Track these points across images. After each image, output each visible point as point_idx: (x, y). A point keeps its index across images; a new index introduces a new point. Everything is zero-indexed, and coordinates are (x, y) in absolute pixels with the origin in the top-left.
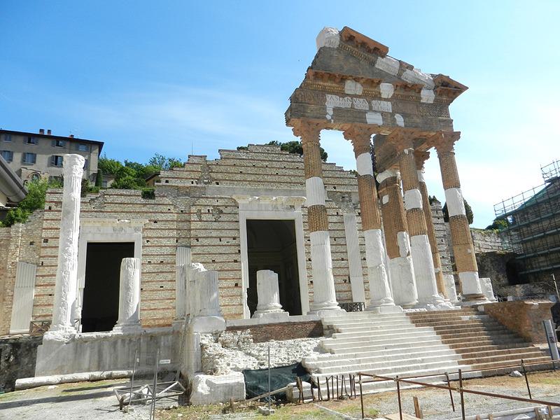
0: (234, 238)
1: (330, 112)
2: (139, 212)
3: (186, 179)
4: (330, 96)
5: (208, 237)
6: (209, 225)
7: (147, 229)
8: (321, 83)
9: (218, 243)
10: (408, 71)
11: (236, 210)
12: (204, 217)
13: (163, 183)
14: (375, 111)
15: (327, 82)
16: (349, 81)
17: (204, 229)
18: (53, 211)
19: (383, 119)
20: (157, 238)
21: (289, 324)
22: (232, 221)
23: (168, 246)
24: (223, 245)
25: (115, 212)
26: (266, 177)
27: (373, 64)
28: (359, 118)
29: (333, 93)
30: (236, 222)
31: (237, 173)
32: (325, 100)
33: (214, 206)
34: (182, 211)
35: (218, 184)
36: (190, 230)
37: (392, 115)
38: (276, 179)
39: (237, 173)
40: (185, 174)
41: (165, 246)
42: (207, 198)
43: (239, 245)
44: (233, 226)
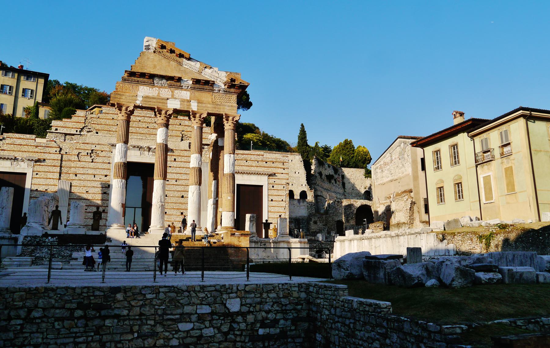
0: (106, 176)
1: (141, 99)
2: (32, 152)
4: (142, 87)
5: (85, 174)
6: (86, 165)
7: (37, 165)
8: (134, 78)
9: (93, 178)
11: (109, 154)
12: (82, 159)
13: (53, 129)
14: (176, 98)
16: (156, 78)
17: (82, 168)
20: (44, 172)
21: (85, 236)
22: (106, 163)
23: (53, 179)
24: (96, 181)
25: (13, 151)
26: (138, 129)
27: (180, 64)
28: (162, 103)
29: (144, 83)
30: (109, 163)
31: (115, 125)
33: (92, 150)
34: (66, 153)
35: (97, 133)
36: (71, 167)
38: (146, 131)
39: (115, 125)
40: (70, 125)
41: (50, 179)
42: (88, 144)
44: (106, 166)
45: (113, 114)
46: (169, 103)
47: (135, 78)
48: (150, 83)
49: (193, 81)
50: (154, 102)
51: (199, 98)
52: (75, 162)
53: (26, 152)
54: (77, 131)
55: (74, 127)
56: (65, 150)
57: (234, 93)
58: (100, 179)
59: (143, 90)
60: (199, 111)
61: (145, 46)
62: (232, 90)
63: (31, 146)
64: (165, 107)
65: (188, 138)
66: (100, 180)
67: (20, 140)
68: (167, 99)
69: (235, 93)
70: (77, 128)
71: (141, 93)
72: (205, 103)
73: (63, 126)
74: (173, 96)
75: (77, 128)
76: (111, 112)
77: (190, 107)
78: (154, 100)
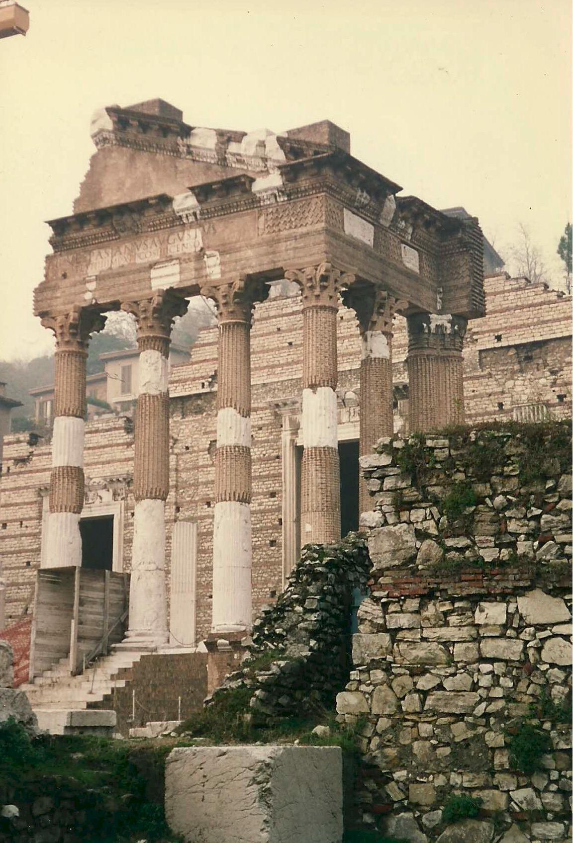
0: (273, 495)
1: (92, 286)
2: (120, 461)
3: (194, 379)
4: (96, 252)
10: (233, 147)
14: (170, 259)
15: (81, 229)
18: (14, 473)
19: (181, 273)
29: (97, 243)
31: (283, 348)
32: (89, 263)
34: (187, 448)
36: (196, 485)
37: (200, 255)
43: (279, 509)
45: (279, 316)
46: (155, 278)
47: (75, 235)
48: (109, 236)
49: (197, 196)
50: (123, 285)
51: (226, 238)
52: (205, 469)
53: (109, 462)
54: (203, 384)
55: (197, 375)
56: (184, 441)
57: (313, 188)
58: (260, 504)
59: (99, 257)
60: (228, 276)
61: (94, 136)
62: (304, 182)
63: (118, 445)
64: (147, 292)
65: (475, 337)
66: (258, 508)
67: (98, 434)
68: (151, 266)
69: (319, 188)
70: (203, 377)
71: (94, 269)
72: (238, 250)
73: (177, 378)
74: (164, 251)
75: (203, 377)
76: (272, 313)
77: (204, 273)
78: (122, 280)
